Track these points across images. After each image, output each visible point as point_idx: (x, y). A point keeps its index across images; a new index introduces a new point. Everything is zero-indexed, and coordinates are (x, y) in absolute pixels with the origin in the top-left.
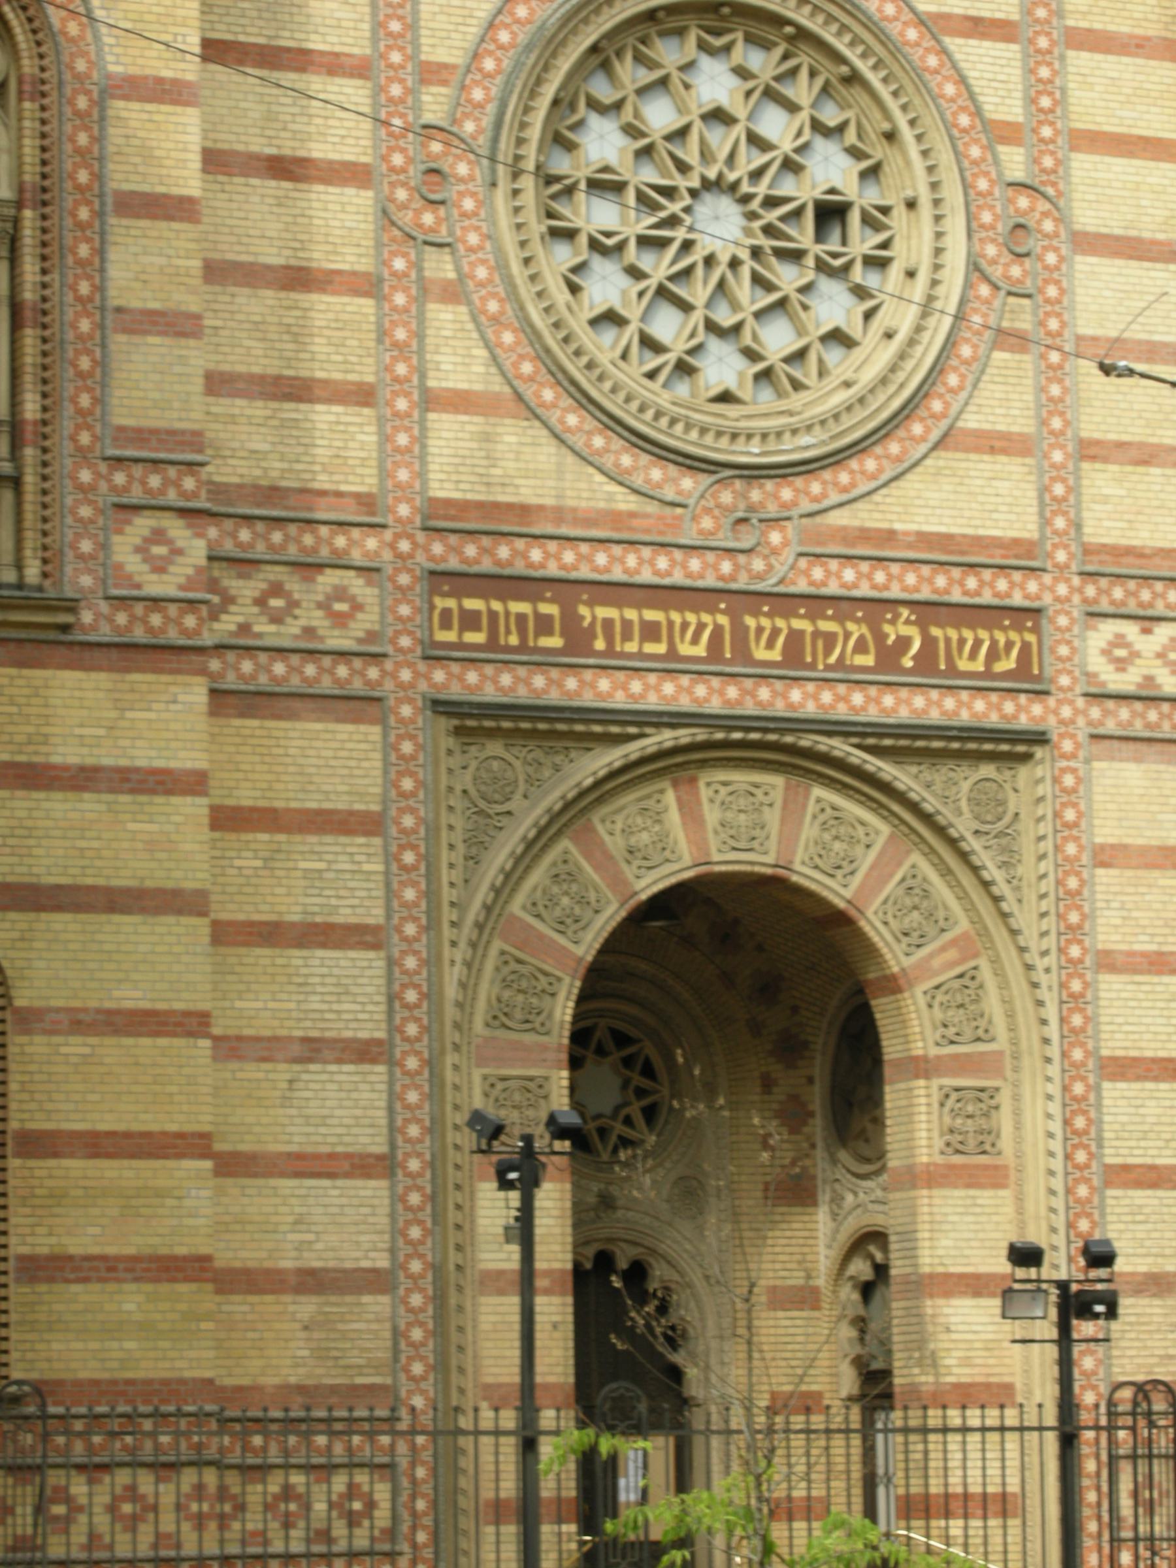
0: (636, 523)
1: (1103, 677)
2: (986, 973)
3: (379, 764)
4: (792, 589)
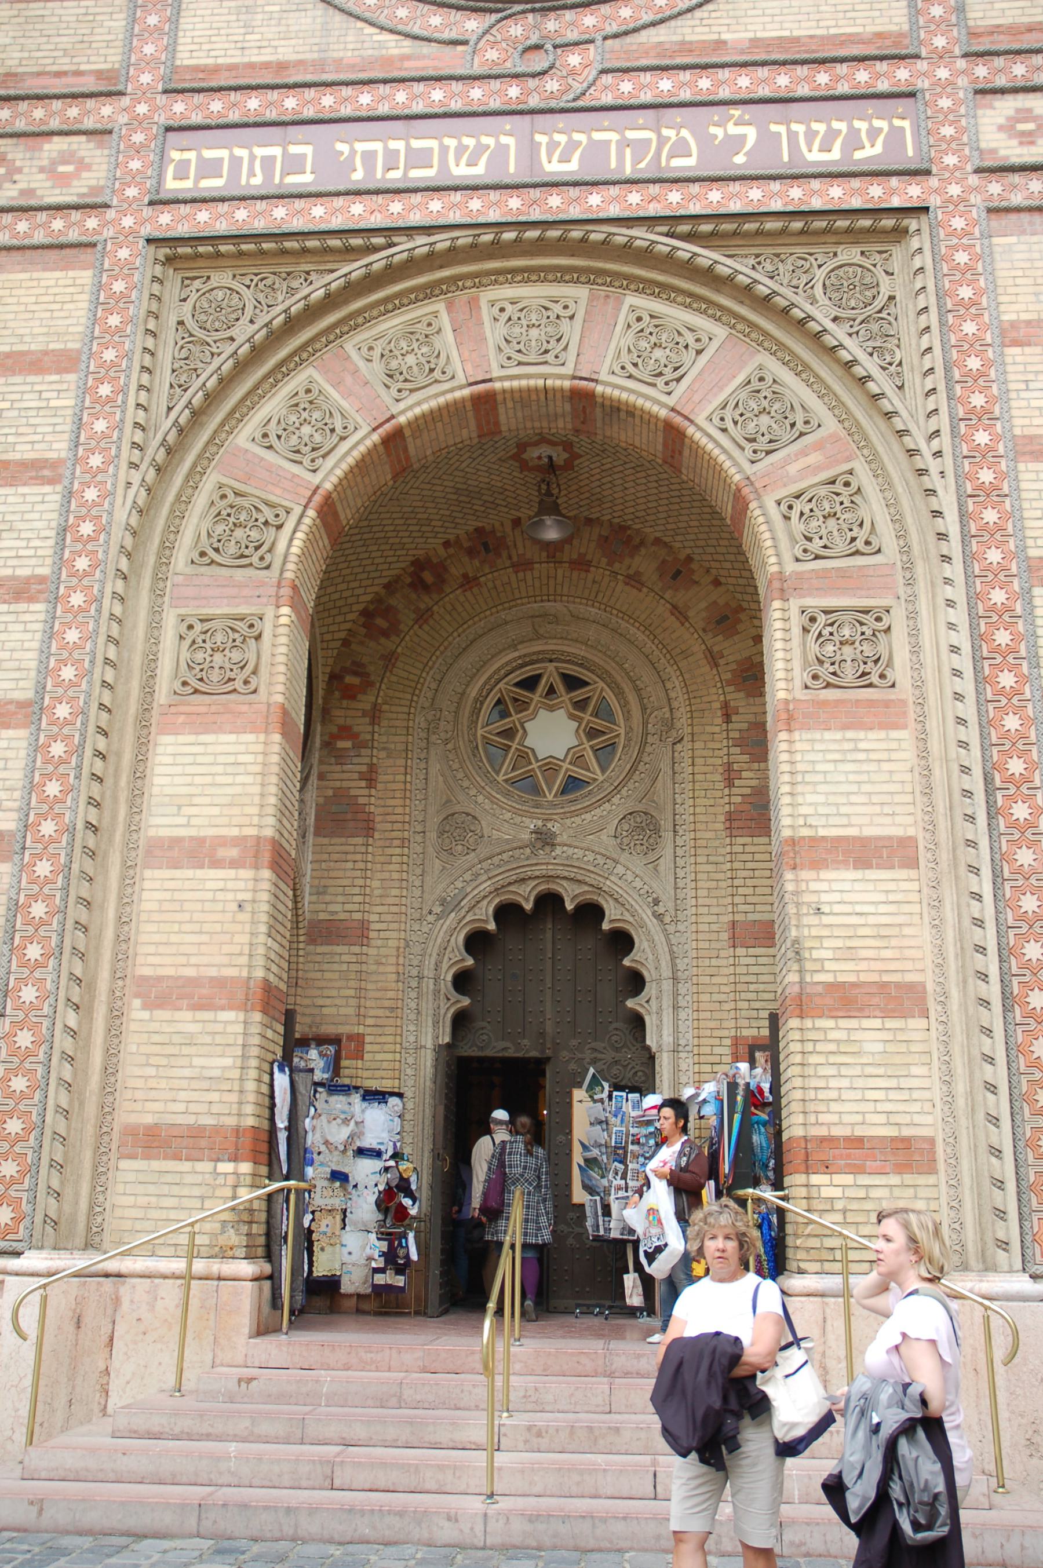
0: (407, 64)
1: (1002, 153)
2: (863, 476)
3: (85, 305)
4: (593, 103)
